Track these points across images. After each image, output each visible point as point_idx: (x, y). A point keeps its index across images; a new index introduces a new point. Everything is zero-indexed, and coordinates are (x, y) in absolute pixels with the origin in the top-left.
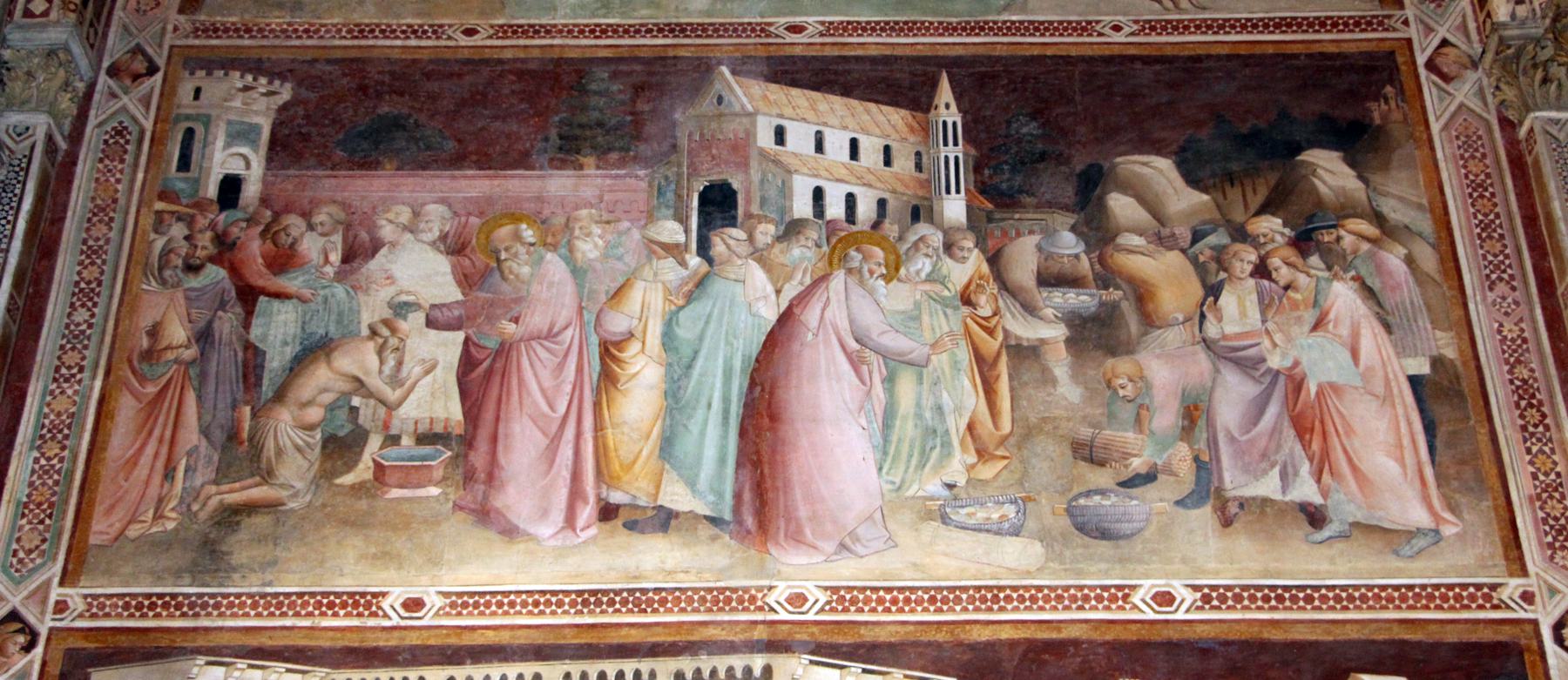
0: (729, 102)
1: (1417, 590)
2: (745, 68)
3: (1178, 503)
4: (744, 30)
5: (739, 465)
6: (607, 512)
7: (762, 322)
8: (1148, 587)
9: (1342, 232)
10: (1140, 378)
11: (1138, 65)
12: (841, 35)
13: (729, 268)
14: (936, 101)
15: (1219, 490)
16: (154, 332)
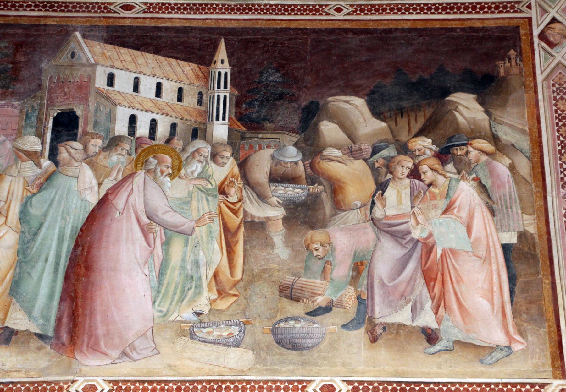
0: (79, 56)
1: (492, 386)
2: (92, 33)
3: (344, 326)
4: (93, 8)
5: (62, 299)
7: (87, 205)
9: (470, 148)
10: (328, 244)
11: (350, 35)
12: (157, 12)
13: (70, 169)
14: (215, 59)
15: (371, 319)
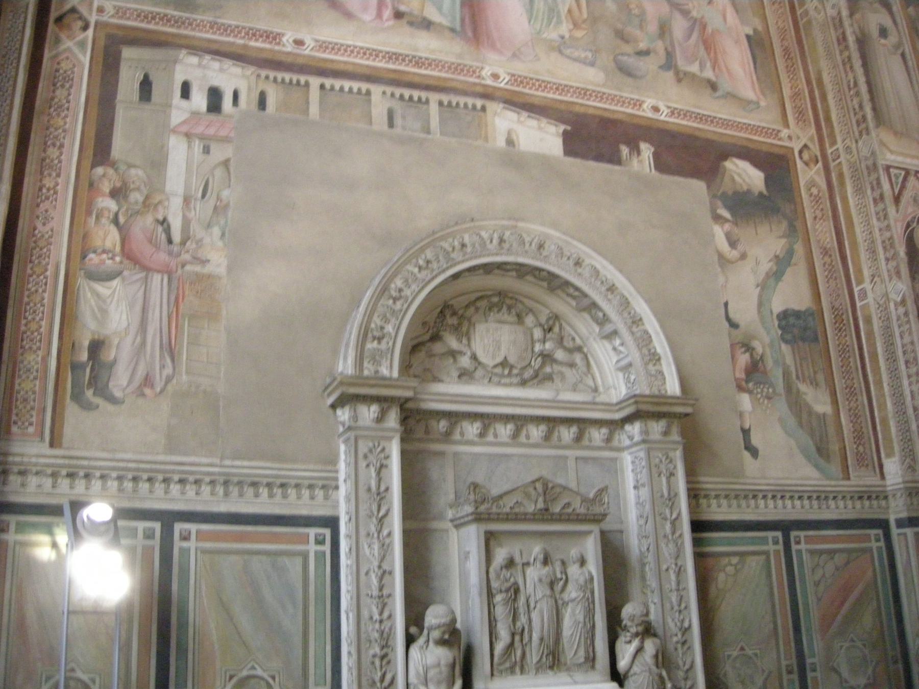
3: (661, 67)
6: (398, 15)
8: (649, 102)
15: (676, 66)
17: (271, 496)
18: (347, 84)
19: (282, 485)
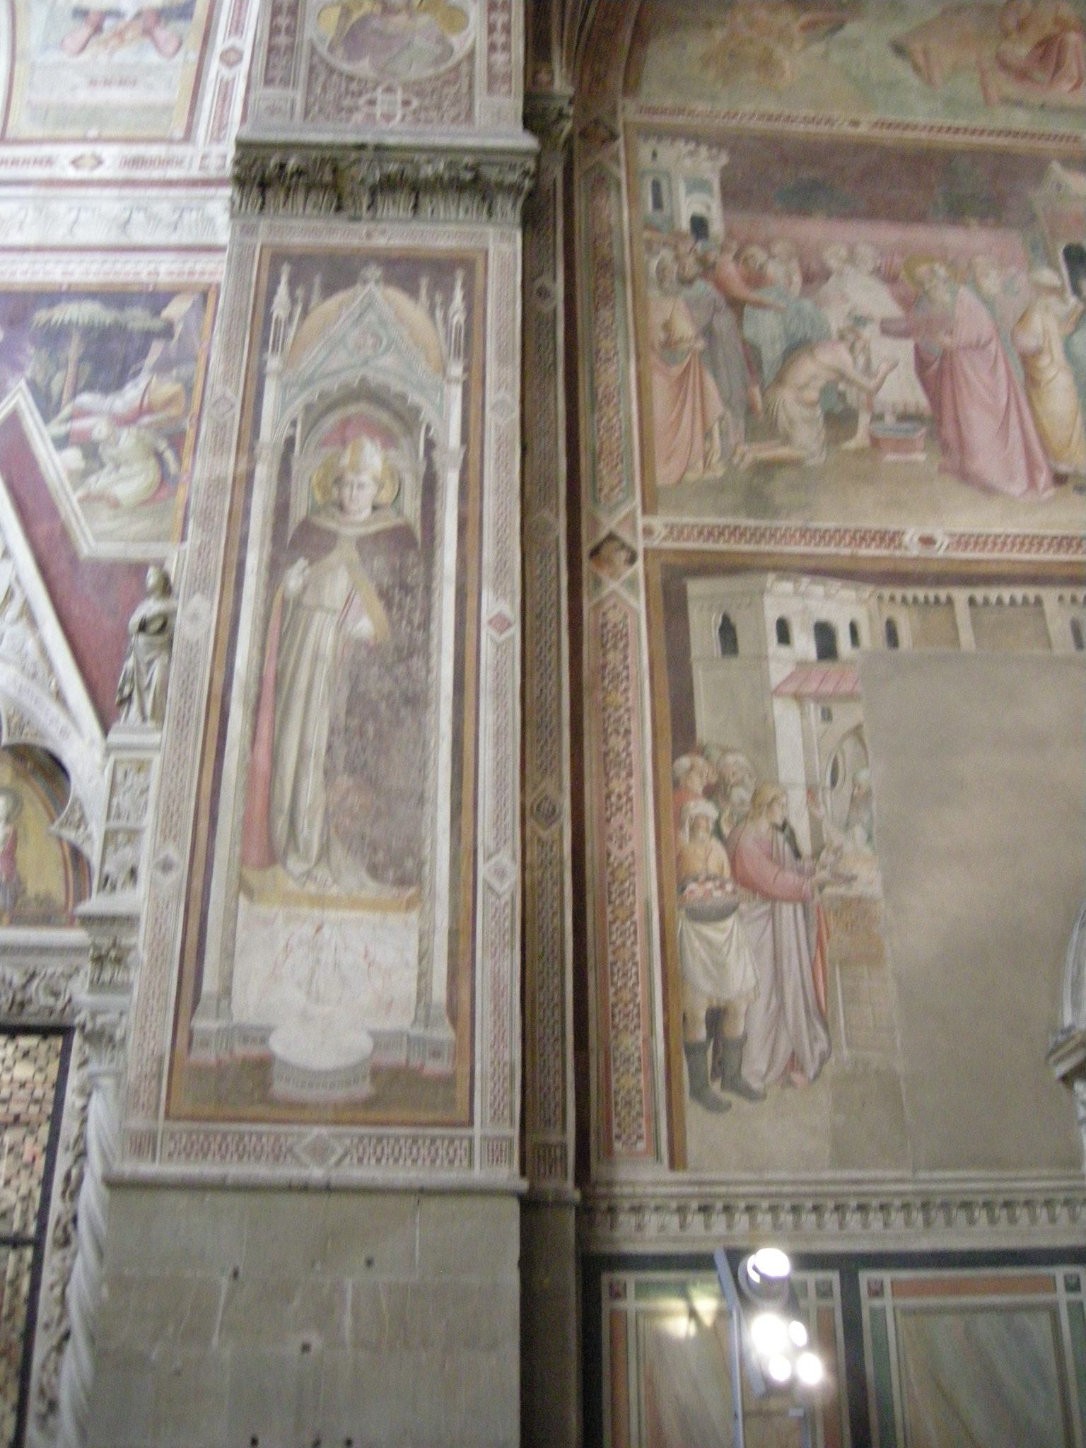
6: (1059, 479)
16: (667, 326)
17: (993, 1221)
18: (1006, 593)
19: (1007, 1205)
